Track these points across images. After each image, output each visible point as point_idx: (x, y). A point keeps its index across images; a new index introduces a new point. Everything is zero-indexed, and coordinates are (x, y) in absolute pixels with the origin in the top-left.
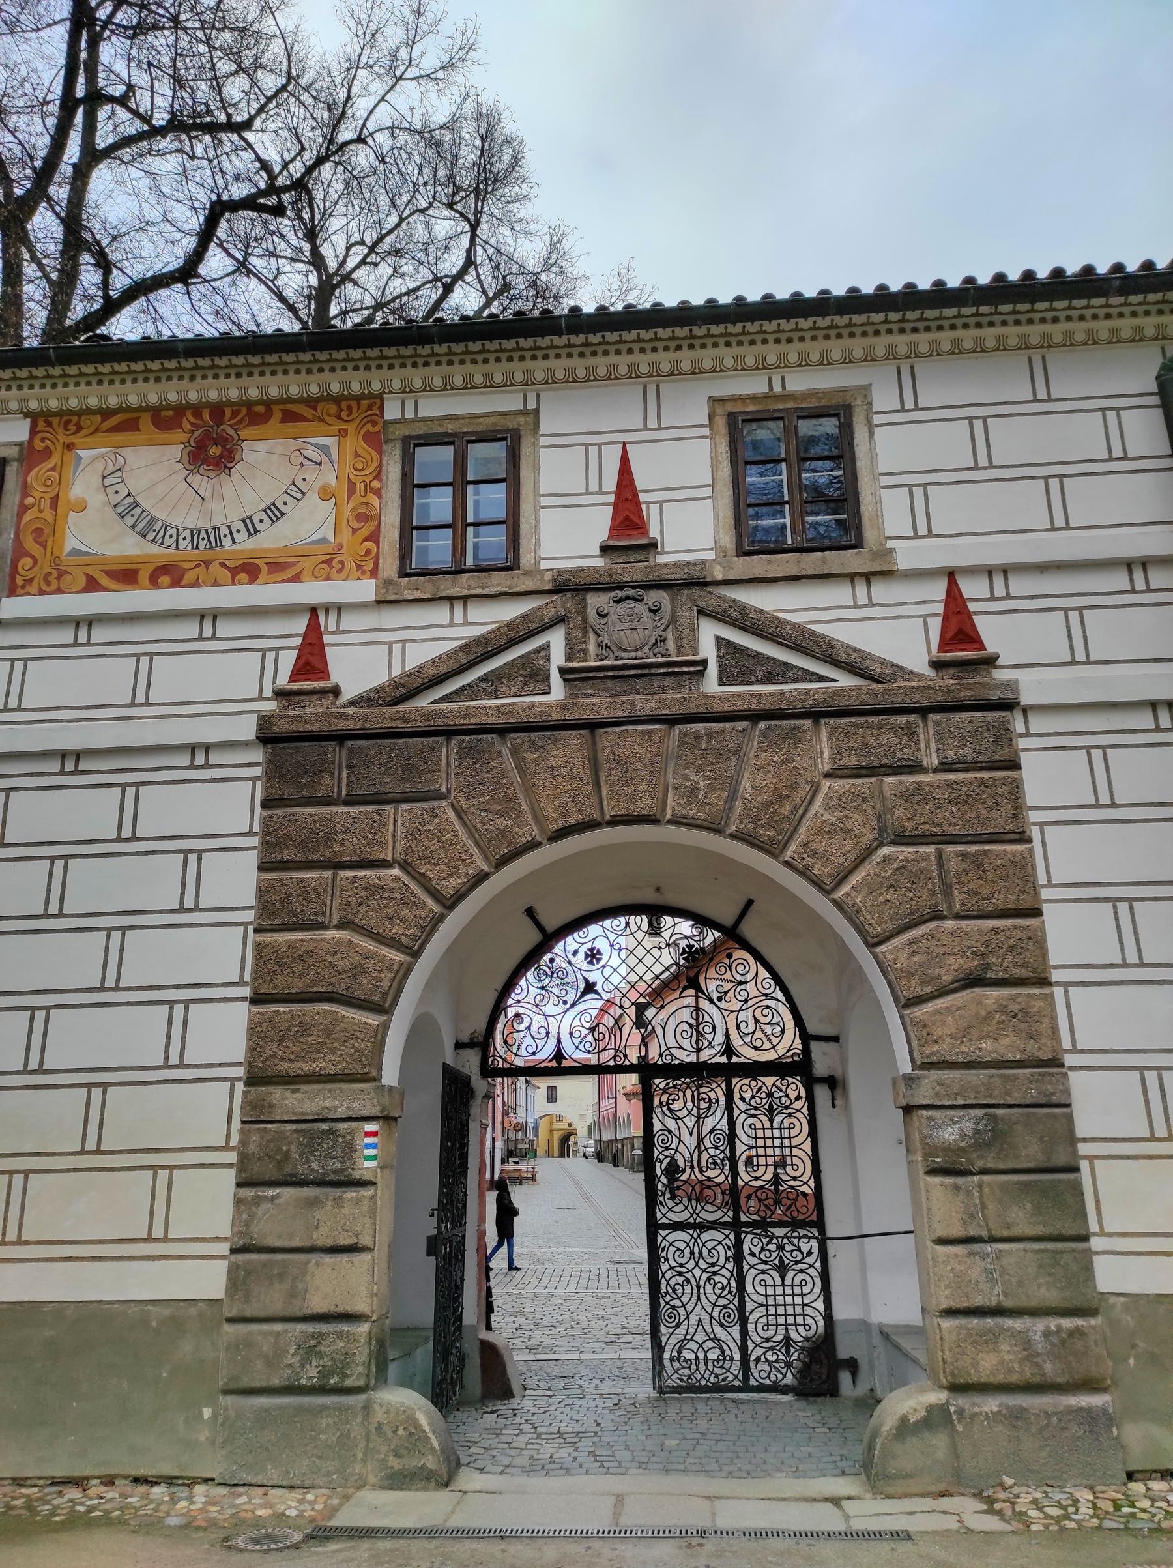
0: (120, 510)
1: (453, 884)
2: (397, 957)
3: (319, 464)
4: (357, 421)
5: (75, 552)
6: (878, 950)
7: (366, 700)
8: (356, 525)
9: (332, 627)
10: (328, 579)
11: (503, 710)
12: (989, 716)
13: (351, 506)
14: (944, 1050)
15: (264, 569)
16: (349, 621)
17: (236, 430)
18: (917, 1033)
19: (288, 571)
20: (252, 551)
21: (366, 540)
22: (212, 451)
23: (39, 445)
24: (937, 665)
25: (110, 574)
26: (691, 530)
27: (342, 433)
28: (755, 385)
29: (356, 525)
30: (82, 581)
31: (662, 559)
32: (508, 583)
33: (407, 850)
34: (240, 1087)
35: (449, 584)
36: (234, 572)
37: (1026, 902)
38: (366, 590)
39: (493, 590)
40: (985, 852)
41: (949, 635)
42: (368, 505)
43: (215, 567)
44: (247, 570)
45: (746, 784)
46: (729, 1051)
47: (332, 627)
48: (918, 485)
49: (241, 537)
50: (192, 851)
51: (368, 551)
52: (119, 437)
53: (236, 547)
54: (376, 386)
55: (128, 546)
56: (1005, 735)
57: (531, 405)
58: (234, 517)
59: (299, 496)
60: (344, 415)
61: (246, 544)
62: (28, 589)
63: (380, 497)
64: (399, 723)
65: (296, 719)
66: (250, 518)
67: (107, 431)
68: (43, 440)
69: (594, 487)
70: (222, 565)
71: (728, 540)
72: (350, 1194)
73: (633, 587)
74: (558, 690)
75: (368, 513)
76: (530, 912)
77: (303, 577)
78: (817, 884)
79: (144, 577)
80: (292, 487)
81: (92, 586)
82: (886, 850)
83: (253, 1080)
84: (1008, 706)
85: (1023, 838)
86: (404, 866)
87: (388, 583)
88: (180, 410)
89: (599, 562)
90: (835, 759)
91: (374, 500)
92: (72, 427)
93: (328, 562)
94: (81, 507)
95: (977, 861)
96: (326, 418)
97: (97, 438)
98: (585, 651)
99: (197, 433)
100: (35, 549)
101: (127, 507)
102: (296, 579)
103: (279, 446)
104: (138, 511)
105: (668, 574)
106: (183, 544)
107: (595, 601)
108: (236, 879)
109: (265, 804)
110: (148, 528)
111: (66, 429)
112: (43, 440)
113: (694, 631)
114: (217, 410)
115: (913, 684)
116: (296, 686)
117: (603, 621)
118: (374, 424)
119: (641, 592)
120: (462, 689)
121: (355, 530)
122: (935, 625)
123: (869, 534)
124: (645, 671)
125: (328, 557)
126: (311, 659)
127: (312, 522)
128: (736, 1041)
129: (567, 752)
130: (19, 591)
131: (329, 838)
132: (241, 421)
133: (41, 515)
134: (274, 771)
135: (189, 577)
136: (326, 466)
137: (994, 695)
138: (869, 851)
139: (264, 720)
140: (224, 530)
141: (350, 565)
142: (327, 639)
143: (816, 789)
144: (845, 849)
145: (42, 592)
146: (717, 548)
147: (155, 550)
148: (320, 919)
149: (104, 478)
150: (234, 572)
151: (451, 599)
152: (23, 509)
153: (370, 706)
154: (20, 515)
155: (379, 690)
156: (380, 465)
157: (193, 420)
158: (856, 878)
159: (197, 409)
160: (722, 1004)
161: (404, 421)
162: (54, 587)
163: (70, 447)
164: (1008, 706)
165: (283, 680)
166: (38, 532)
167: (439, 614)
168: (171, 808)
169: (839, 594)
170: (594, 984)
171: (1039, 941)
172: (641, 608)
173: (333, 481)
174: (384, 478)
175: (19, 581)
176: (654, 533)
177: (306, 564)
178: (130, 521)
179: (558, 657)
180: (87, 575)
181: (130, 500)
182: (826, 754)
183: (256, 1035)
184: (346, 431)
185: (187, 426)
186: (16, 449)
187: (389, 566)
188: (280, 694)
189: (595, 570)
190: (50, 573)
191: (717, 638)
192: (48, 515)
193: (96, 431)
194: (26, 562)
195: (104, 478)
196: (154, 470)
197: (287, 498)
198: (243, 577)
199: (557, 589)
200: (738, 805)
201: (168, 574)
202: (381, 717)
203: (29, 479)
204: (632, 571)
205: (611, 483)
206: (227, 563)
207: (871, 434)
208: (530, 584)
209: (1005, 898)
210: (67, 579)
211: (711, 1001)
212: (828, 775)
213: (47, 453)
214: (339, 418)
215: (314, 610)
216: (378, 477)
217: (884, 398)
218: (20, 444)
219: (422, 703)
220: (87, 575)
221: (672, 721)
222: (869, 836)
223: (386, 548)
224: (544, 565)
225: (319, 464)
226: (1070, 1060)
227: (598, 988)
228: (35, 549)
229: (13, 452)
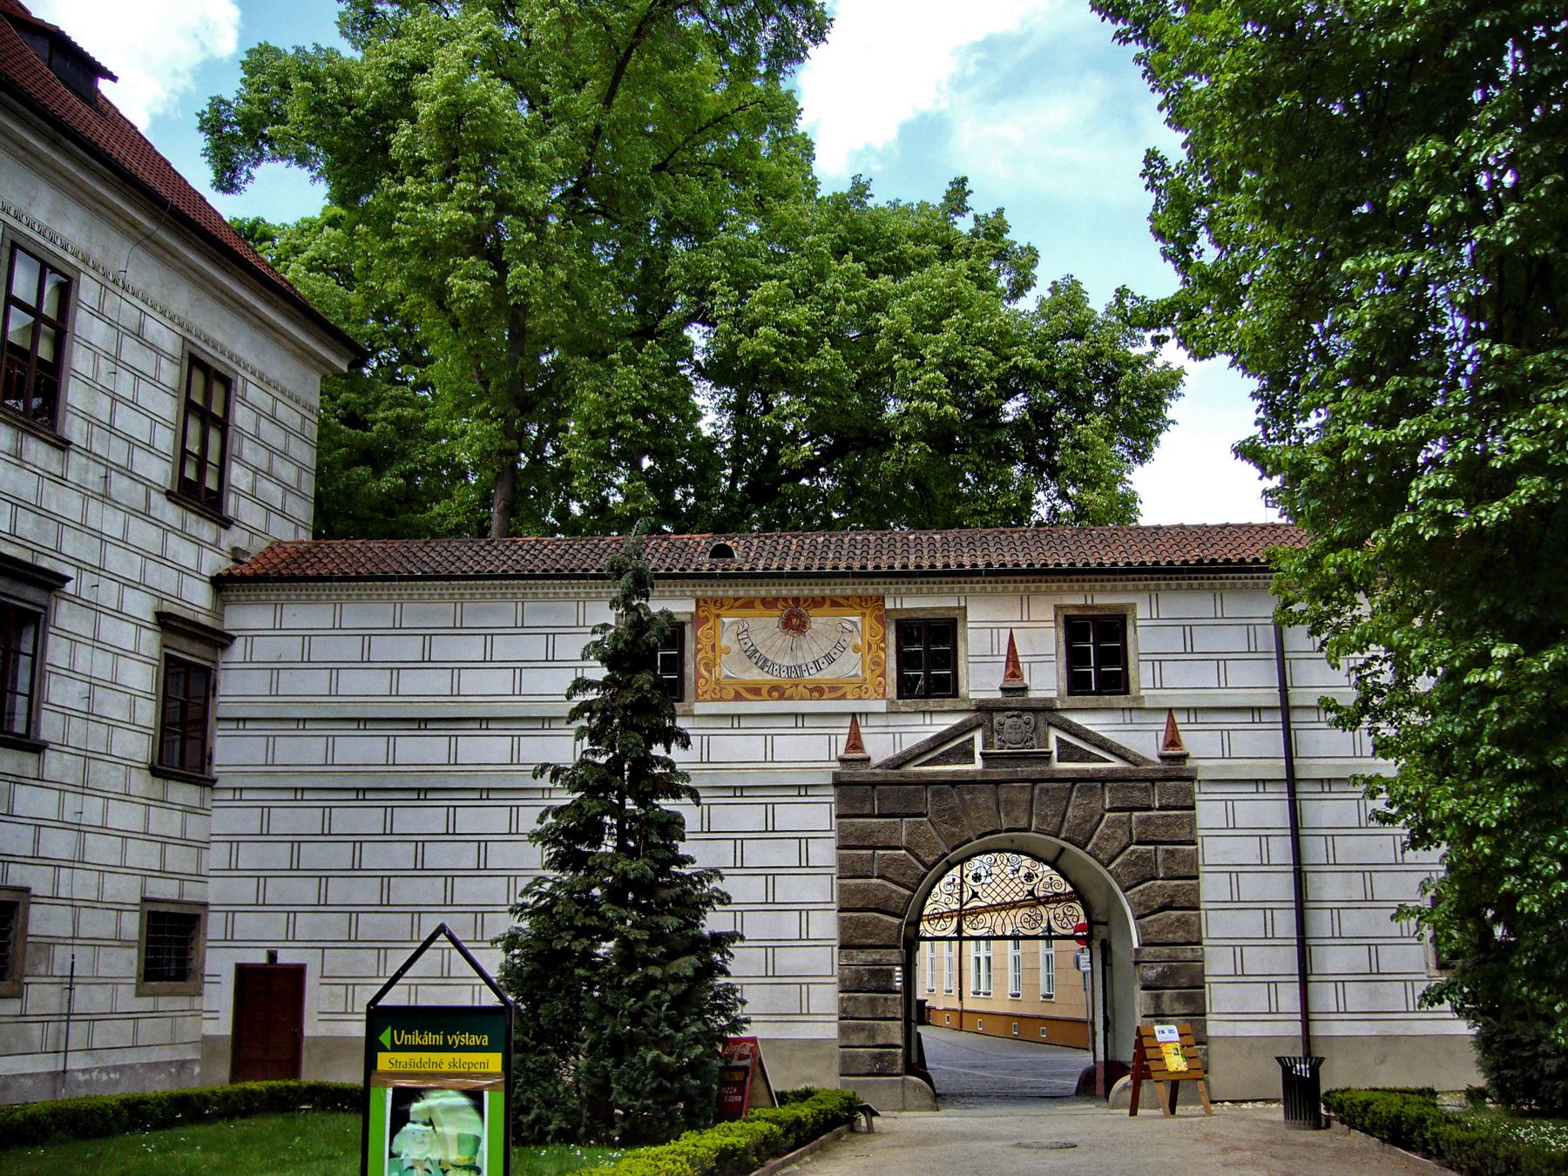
1: (932, 859)
2: (908, 893)
10: (860, 698)
11: (955, 773)
12: (1183, 784)
14: (1151, 938)
16: (872, 721)
18: (1142, 930)
22: (794, 623)
23: (702, 614)
24: (1162, 757)
25: (749, 690)
27: (863, 615)
28: (1079, 600)
31: (1031, 695)
33: (909, 842)
34: (836, 950)
36: (811, 691)
37: (1194, 873)
38: (881, 706)
44: (818, 691)
45: (1070, 813)
46: (1049, 929)
48: (1158, 660)
49: (813, 671)
50: (804, 838)
52: (744, 612)
54: (881, 591)
55: (755, 675)
56: (1191, 794)
58: (809, 660)
61: (814, 676)
65: (852, 775)
71: (1063, 686)
72: (891, 996)
74: (979, 764)
78: (1101, 863)
79: (764, 692)
81: (738, 697)
83: (841, 947)
84: (1192, 779)
85: (1194, 843)
88: (776, 599)
89: (999, 695)
95: (1172, 853)
97: (733, 612)
100: (705, 674)
101: (752, 653)
102: (843, 697)
103: (830, 620)
105: (1033, 705)
107: (998, 718)
108: (825, 852)
109: (838, 817)
110: (763, 664)
113: (1047, 734)
114: (796, 600)
122: (1162, 735)
123: (1132, 686)
127: (849, 666)
128: (1053, 924)
129: (983, 797)
134: (841, 800)
138: (1125, 848)
139: (835, 774)
141: (871, 689)
142: (862, 730)
143: (1102, 816)
144: (1114, 846)
145: (713, 700)
150: (811, 691)
151: (924, 712)
155: (891, 760)
158: (1118, 860)
159: (785, 599)
163: (718, 616)
164: (1192, 779)
165: (841, 753)
166: (707, 665)
167: (919, 719)
168: (792, 815)
169: (1117, 717)
171: (1196, 890)
172: (1020, 721)
176: (1026, 681)
177: (848, 689)
179: (978, 748)
183: (844, 926)
187: (892, 692)
188: (842, 760)
191: (1059, 740)
192: (710, 655)
194: (702, 681)
196: (765, 628)
198: (816, 694)
199: (978, 710)
200: (1066, 825)
201: (777, 692)
202: (893, 774)
204: (1015, 701)
205: (1004, 651)
208: (965, 706)
209: (1182, 871)
212: (1109, 810)
213: (706, 619)
215: (854, 715)
216: (883, 640)
217: (1142, 612)
219: (912, 768)
221: (1035, 782)
222: (1125, 840)
226: (1205, 942)
229: (687, 618)
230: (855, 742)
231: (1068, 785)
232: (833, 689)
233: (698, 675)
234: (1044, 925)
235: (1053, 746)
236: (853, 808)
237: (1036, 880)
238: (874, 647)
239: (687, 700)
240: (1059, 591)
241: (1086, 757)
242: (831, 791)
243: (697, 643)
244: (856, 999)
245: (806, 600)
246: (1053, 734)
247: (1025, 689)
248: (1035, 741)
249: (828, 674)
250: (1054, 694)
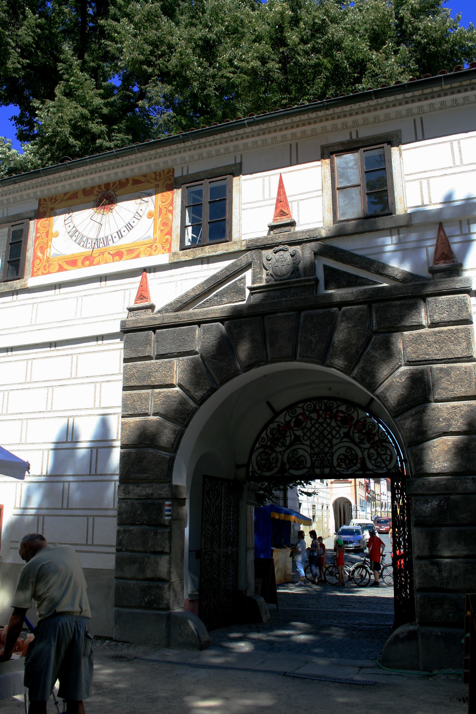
0: (70, 234)
3: (147, 202)
4: (163, 180)
6: (396, 420)
7: (165, 310)
8: (162, 228)
10: (150, 255)
13: (160, 220)
15: (125, 253)
17: (114, 192)
19: (135, 253)
20: (120, 246)
21: (166, 235)
29: (162, 228)
30: (57, 267)
32: (226, 248)
35: (200, 251)
36: (113, 255)
40: (451, 368)
41: (438, 256)
42: (168, 218)
43: (106, 254)
44: (119, 255)
51: (167, 240)
52: (70, 202)
53: (115, 245)
54: (170, 163)
56: (464, 306)
57: (238, 161)
59: (139, 218)
60: (158, 178)
61: (119, 243)
62: (38, 273)
63: (172, 214)
64: (177, 320)
65: (135, 321)
66: (120, 231)
67: (67, 200)
68: (43, 208)
69: (267, 197)
70: (109, 253)
73: (283, 245)
75: (167, 222)
76: (268, 403)
77: (142, 256)
79: (79, 263)
80: (137, 214)
81: (61, 269)
87: (175, 254)
90: (378, 323)
92: (53, 201)
93: (151, 247)
94: (57, 235)
96: (151, 180)
98: (261, 278)
99: (99, 195)
100: (40, 255)
102: (138, 256)
104: (77, 233)
111: (51, 202)
112: (43, 208)
115: (418, 283)
116: (136, 306)
117: (269, 262)
118: (170, 180)
119: (287, 246)
120: (207, 301)
121: (162, 231)
124: (288, 286)
125: (151, 244)
126: (142, 294)
130: (35, 274)
131: (149, 375)
132: (117, 186)
133: (43, 241)
135: (96, 261)
139: (123, 323)
140: (110, 238)
141: (159, 246)
145: (43, 274)
147: (83, 250)
148: (147, 411)
149: (65, 221)
150: (113, 255)
152: (37, 238)
153: (166, 312)
154: (35, 241)
156: (173, 199)
157: (98, 190)
160: (362, 446)
161: (182, 176)
162: (47, 271)
166: (42, 248)
170: (300, 436)
174: (174, 205)
175: (35, 270)
177: (142, 249)
178: (74, 238)
179: (249, 283)
180: (59, 265)
181: (74, 229)
182: (374, 322)
184: (158, 185)
185: (95, 193)
186: (34, 213)
187: (176, 246)
190: (45, 266)
193: (62, 200)
194: (38, 261)
195: (65, 221)
197: (134, 219)
198: (117, 258)
201: (89, 260)
202: (171, 317)
203: (38, 226)
204: (281, 236)
205: (275, 194)
206: (111, 252)
207: (401, 155)
210: (52, 266)
212: (376, 332)
214: (156, 179)
216: (171, 204)
218: (35, 211)
220: (59, 265)
221: (299, 310)
223: (174, 237)
224: (243, 238)
225: (147, 202)
227: (301, 438)
228: (40, 255)
230: (142, 294)
232: (130, 251)
233: (35, 257)
236: (136, 351)
238: (164, 210)
239: (25, 277)
243: (37, 232)
244: (130, 531)
245: (114, 184)
247: (292, 224)
249: (129, 239)
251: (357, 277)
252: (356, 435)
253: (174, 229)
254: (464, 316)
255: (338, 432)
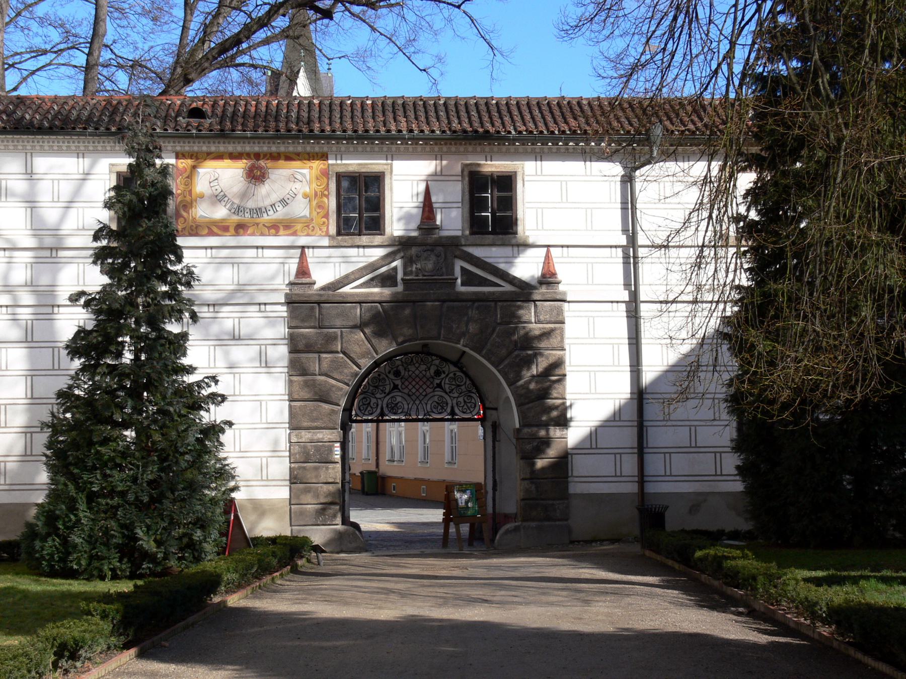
5: (202, 216)
9: (311, 255)
25: (218, 227)
26: (451, 220)
39: (376, 244)
47: (311, 255)
51: (324, 223)
54: (325, 149)
56: (560, 312)
72: (331, 466)
81: (211, 233)
82: (516, 353)
84: (564, 301)
85: (563, 349)
86: (344, 353)
90: (502, 318)
91: (325, 200)
104: (226, 199)
106: (247, 215)
113: (453, 265)
114: (257, 156)
128: (457, 411)
136: (305, 182)
137: (558, 297)
138: (510, 353)
139: (287, 295)
140: (264, 210)
146: (463, 230)
151: (358, 247)
156: (328, 184)
158: (506, 362)
165: (292, 278)
173: (308, 190)
187: (333, 230)
189: (415, 238)
191: (462, 268)
198: (273, 231)
211: (446, 393)
212: (499, 324)
215: (303, 247)
219: (347, 289)
221: (444, 301)
230: (303, 271)
231: (469, 304)
234: (449, 410)
235: (458, 272)
237: (443, 376)
240: (466, 152)
241: (484, 282)
242: (285, 308)
244: (304, 468)
246: (459, 264)
248: (444, 269)
250: (459, 233)
251: (486, 279)
252: (447, 386)
253: (330, 213)
254: (560, 318)
255: (432, 383)
